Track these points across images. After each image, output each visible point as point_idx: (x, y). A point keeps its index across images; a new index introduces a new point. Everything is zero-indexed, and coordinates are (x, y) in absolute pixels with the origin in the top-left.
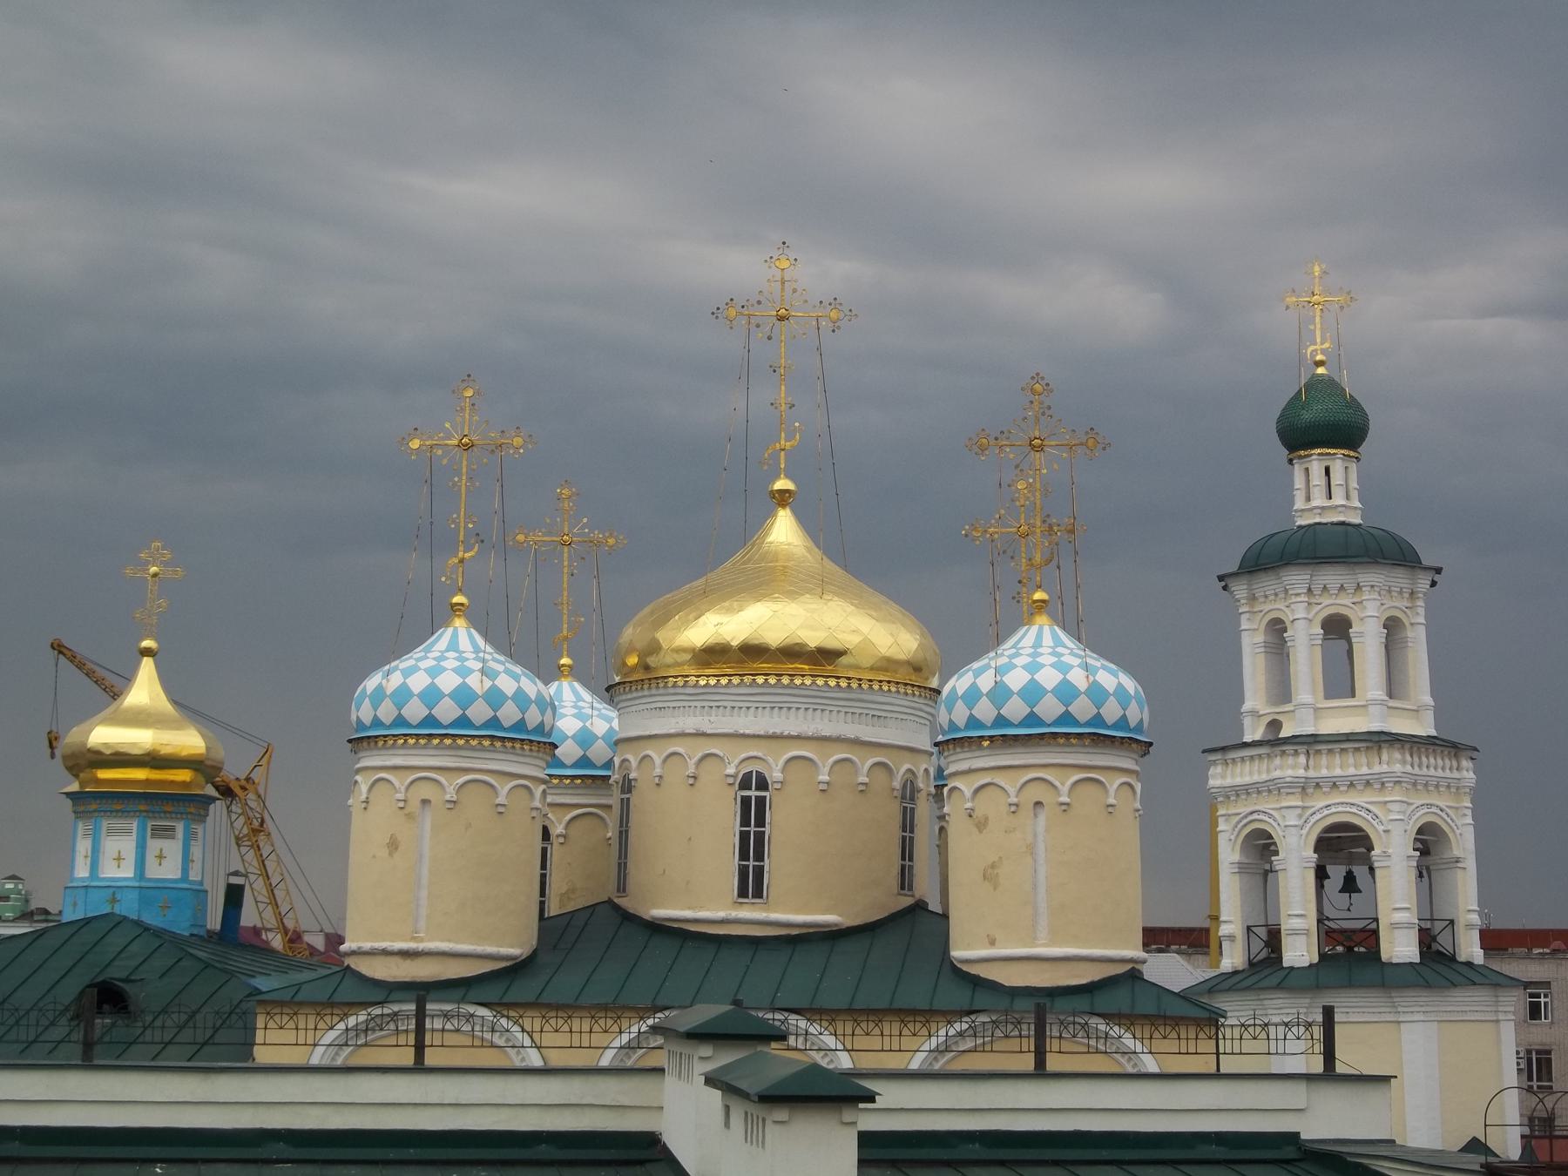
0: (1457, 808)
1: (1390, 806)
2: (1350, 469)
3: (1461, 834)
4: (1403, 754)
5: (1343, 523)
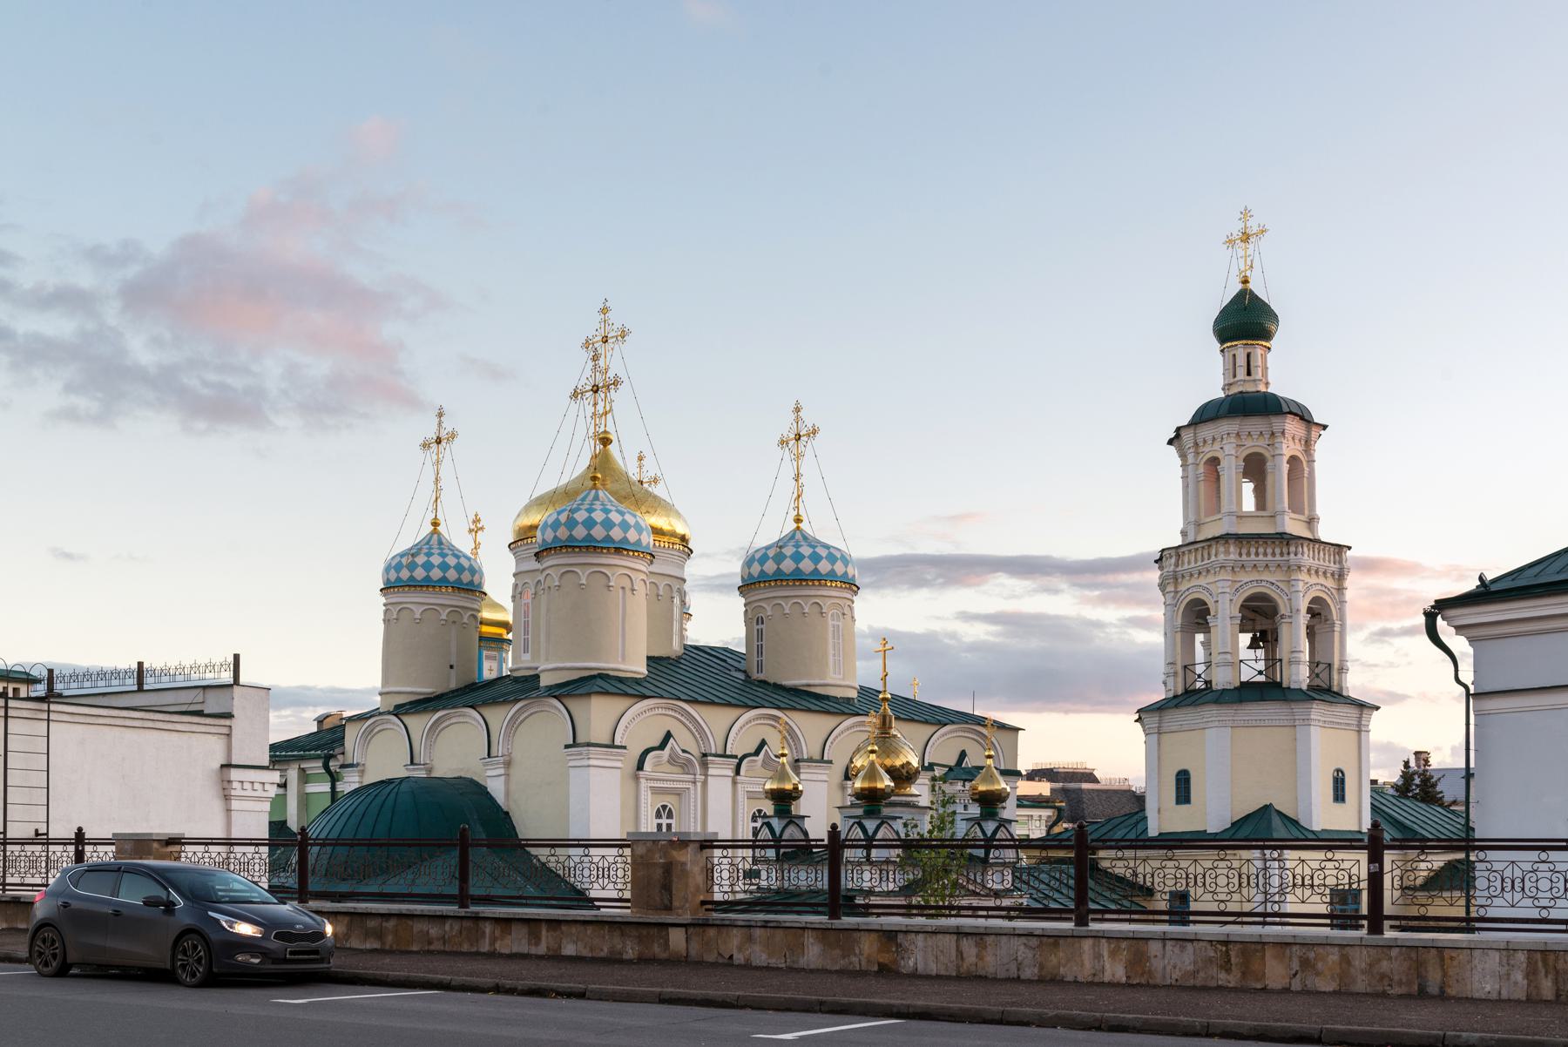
5: (1241, 392)
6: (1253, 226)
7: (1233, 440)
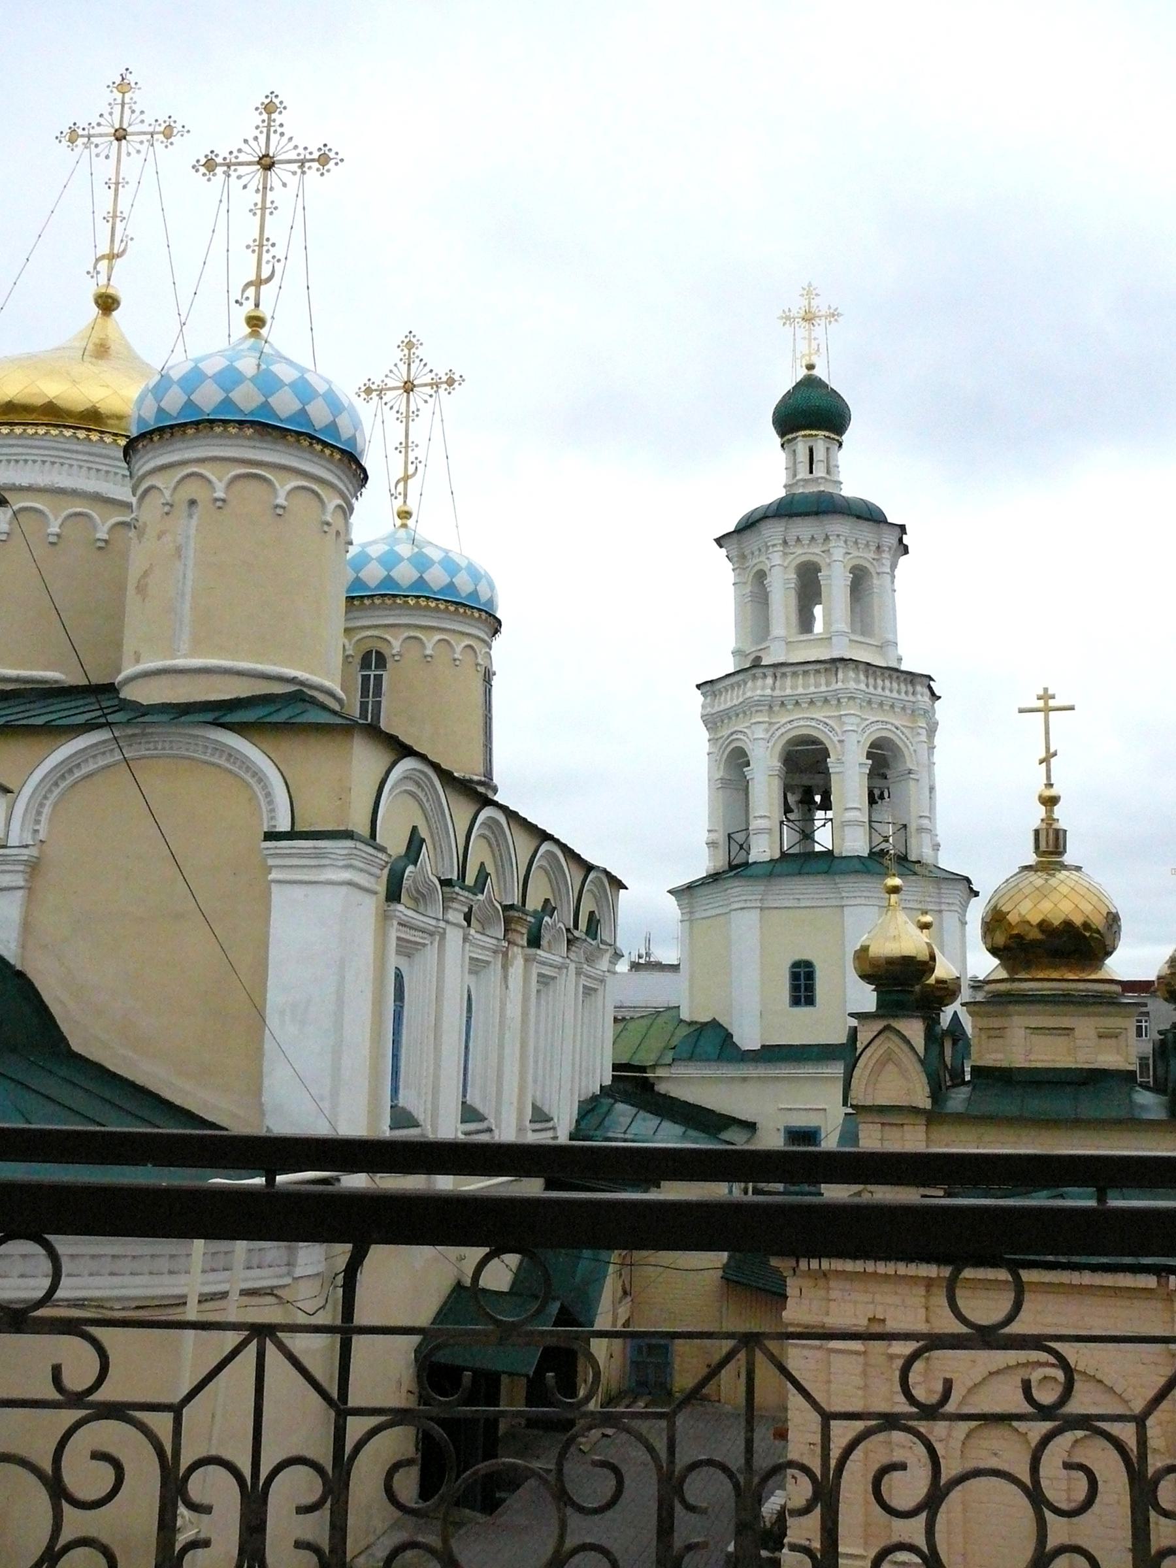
0: (912, 728)
1: (844, 719)
2: (831, 451)
3: (915, 751)
4: (857, 675)
6: (821, 305)
7: (842, 544)
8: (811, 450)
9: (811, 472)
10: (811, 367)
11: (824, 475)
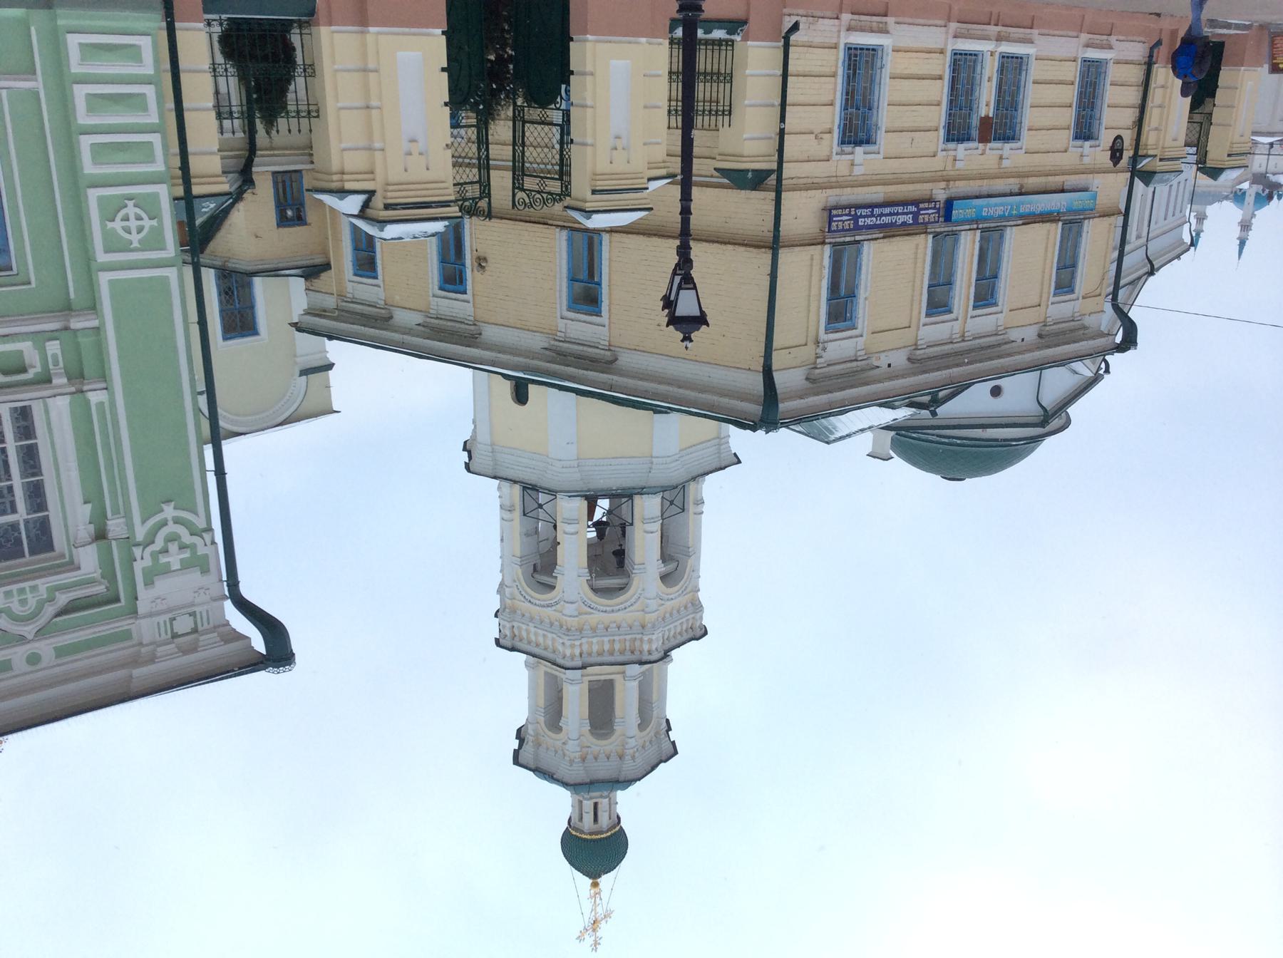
8: (596, 819)
9: (596, 805)
10: (595, 885)
11: (585, 802)
